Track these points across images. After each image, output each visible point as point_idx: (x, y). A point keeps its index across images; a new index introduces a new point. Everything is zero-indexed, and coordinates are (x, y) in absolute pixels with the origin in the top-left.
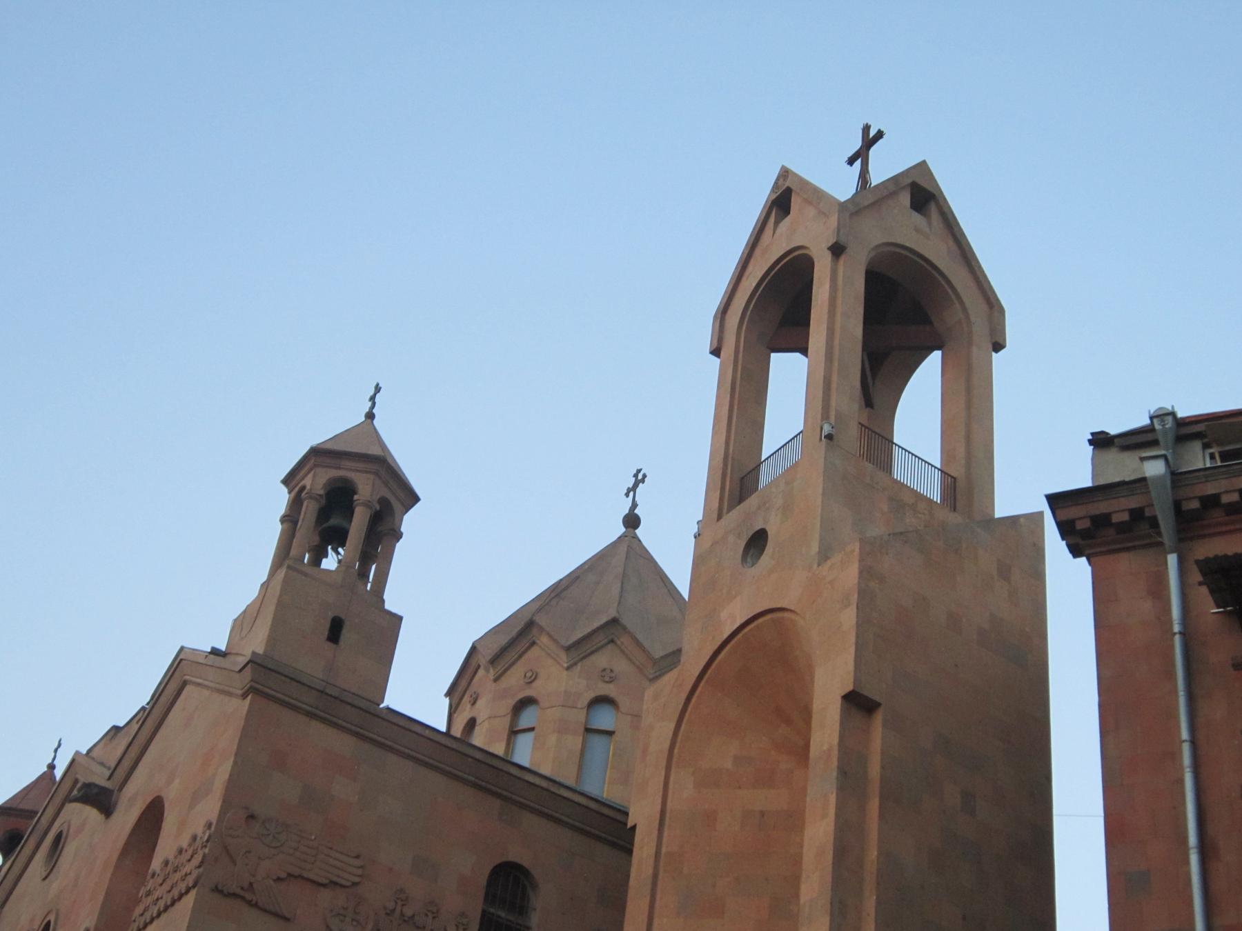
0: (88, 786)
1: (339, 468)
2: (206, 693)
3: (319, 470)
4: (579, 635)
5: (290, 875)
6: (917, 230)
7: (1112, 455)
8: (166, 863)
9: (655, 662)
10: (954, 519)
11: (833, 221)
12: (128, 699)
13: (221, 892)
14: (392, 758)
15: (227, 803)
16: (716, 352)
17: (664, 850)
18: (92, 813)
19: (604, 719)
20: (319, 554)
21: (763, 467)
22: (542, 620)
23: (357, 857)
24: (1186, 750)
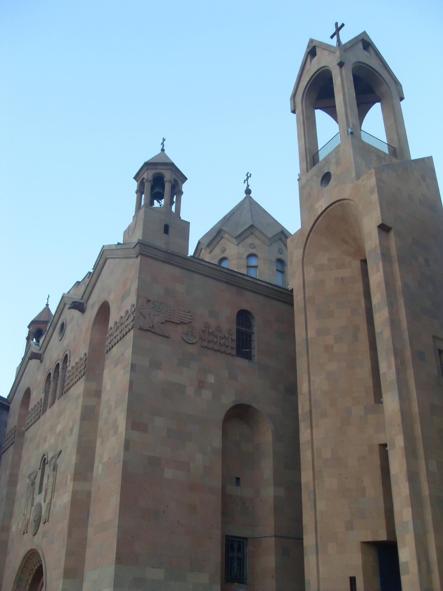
0: (74, 302)
1: (156, 169)
2: (118, 260)
3: (149, 171)
5: (166, 321)
8: (116, 323)
9: (269, 239)
11: (338, 53)
13: (143, 329)
15: (138, 297)
16: (294, 112)
17: (307, 296)
18: (76, 313)
19: (253, 262)
20: (152, 203)
21: (320, 152)
22: (224, 228)
23: (189, 312)
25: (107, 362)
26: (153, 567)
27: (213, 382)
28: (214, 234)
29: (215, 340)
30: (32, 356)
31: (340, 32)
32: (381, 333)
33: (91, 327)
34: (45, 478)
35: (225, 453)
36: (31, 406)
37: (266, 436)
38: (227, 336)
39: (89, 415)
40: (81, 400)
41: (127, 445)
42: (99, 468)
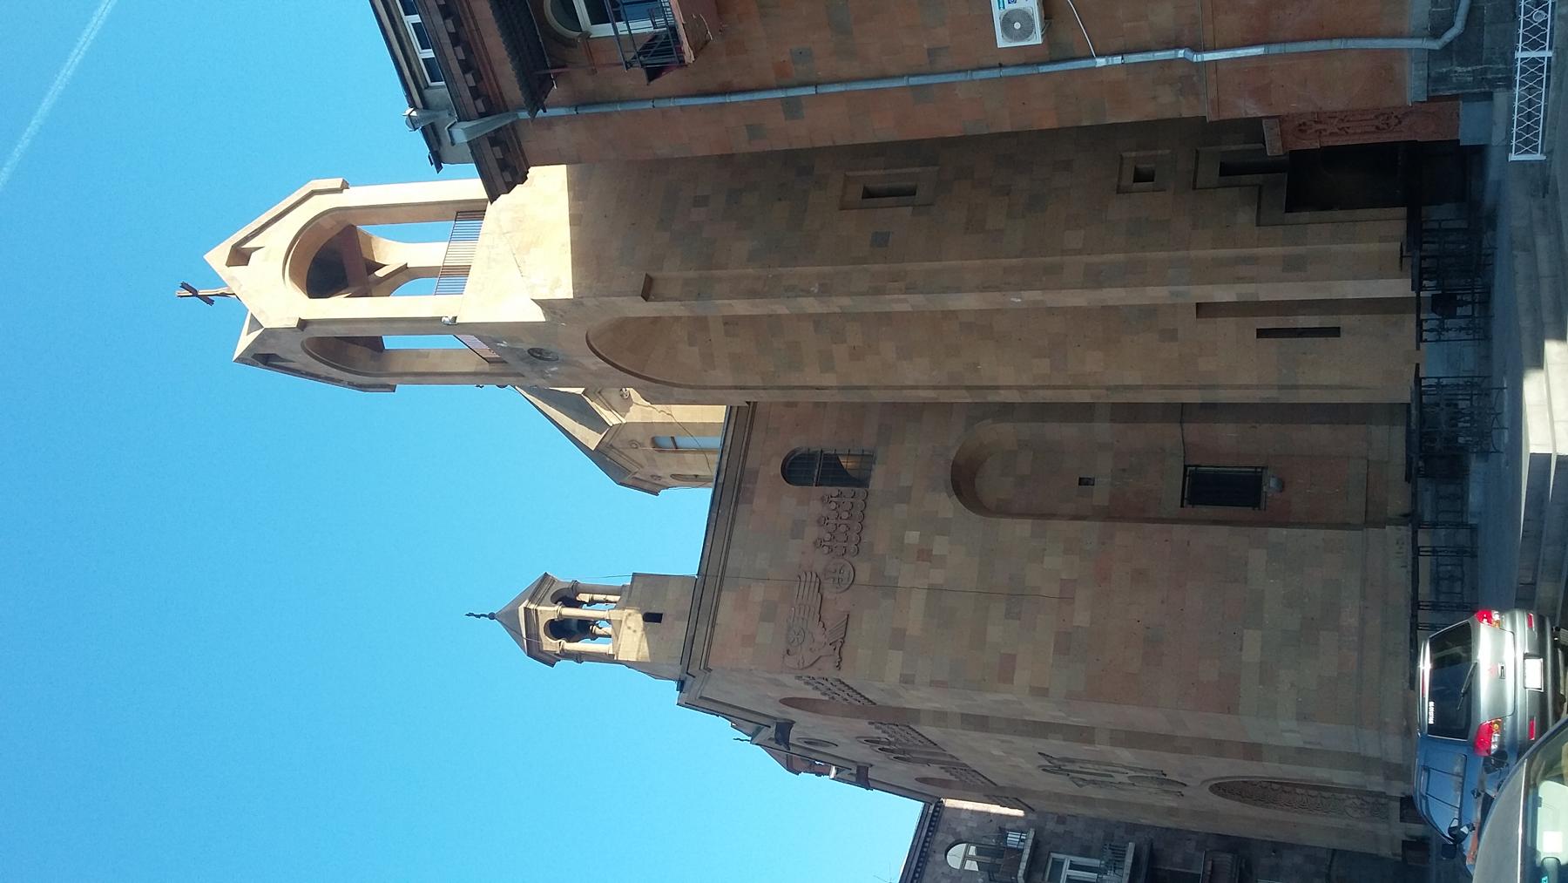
7: (446, 149)
18: (793, 736)
29: (843, 528)
38: (833, 506)
39: (979, 723)
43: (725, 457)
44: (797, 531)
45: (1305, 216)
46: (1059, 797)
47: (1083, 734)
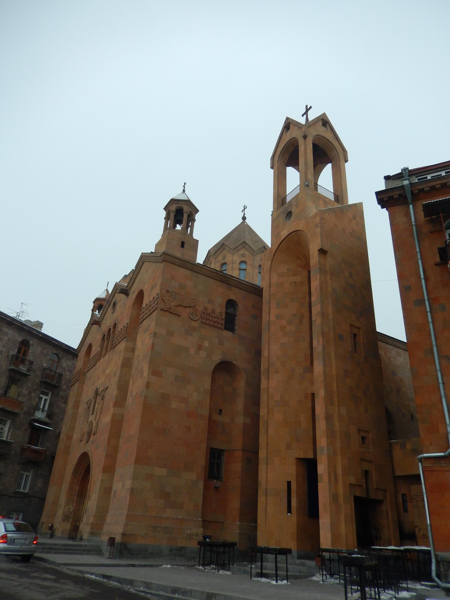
4: (235, 246)
6: (324, 131)
8: (147, 305)
10: (337, 205)
12: (130, 265)
14: (200, 275)
15: (161, 288)
16: (272, 168)
17: (271, 292)
18: (123, 296)
19: (243, 266)
20: (175, 227)
22: (226, 243)
24: (419, 254)
25: (141, 330)
26: (159, 467)
27: (207, 345)
28: (219, 247)
29: (211, 318)
30: (94, 322)
31: (309, 112)
32: (315, 320)
33: (131, 306)
34: (97, 405)
35: (212, 392)
36: (92, 356)
37: (241, 384)
39: (127, 364)
40: (122, 354)
41: (148, 385)
42: (130, 400)
43: (237, 280)
44: (210, 301)
45: (353, 504)
46: (79, 395)
47: (120, 401)
